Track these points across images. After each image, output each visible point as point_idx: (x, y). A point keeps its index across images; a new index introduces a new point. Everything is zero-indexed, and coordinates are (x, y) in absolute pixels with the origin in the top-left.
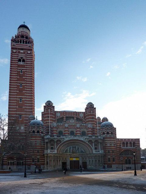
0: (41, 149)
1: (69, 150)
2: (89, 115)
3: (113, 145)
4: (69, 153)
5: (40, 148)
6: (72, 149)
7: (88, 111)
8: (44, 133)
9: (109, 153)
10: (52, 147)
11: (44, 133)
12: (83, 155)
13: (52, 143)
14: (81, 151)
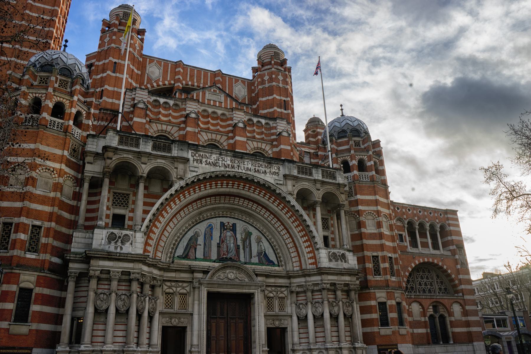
0: (59, 220)
1: (201, 240)
2: (270, 91)
3: (385, 231)
4: (206, 264)
5: (50, 217)
6: (216, 234)
7: (266, 72)
8: (86, 128)
9: (377, 271)
10: (119, 211)
11: (86, 128)
12: (272, 280)
13: (123, 186)
14: (259, 254)
